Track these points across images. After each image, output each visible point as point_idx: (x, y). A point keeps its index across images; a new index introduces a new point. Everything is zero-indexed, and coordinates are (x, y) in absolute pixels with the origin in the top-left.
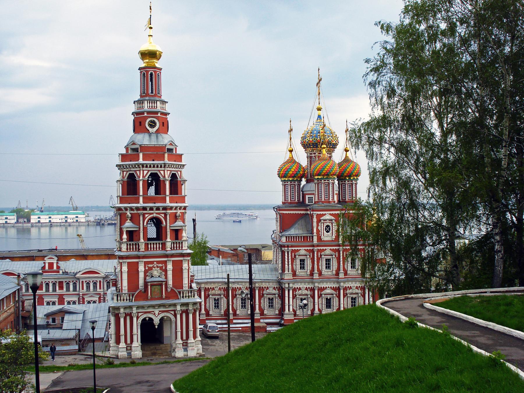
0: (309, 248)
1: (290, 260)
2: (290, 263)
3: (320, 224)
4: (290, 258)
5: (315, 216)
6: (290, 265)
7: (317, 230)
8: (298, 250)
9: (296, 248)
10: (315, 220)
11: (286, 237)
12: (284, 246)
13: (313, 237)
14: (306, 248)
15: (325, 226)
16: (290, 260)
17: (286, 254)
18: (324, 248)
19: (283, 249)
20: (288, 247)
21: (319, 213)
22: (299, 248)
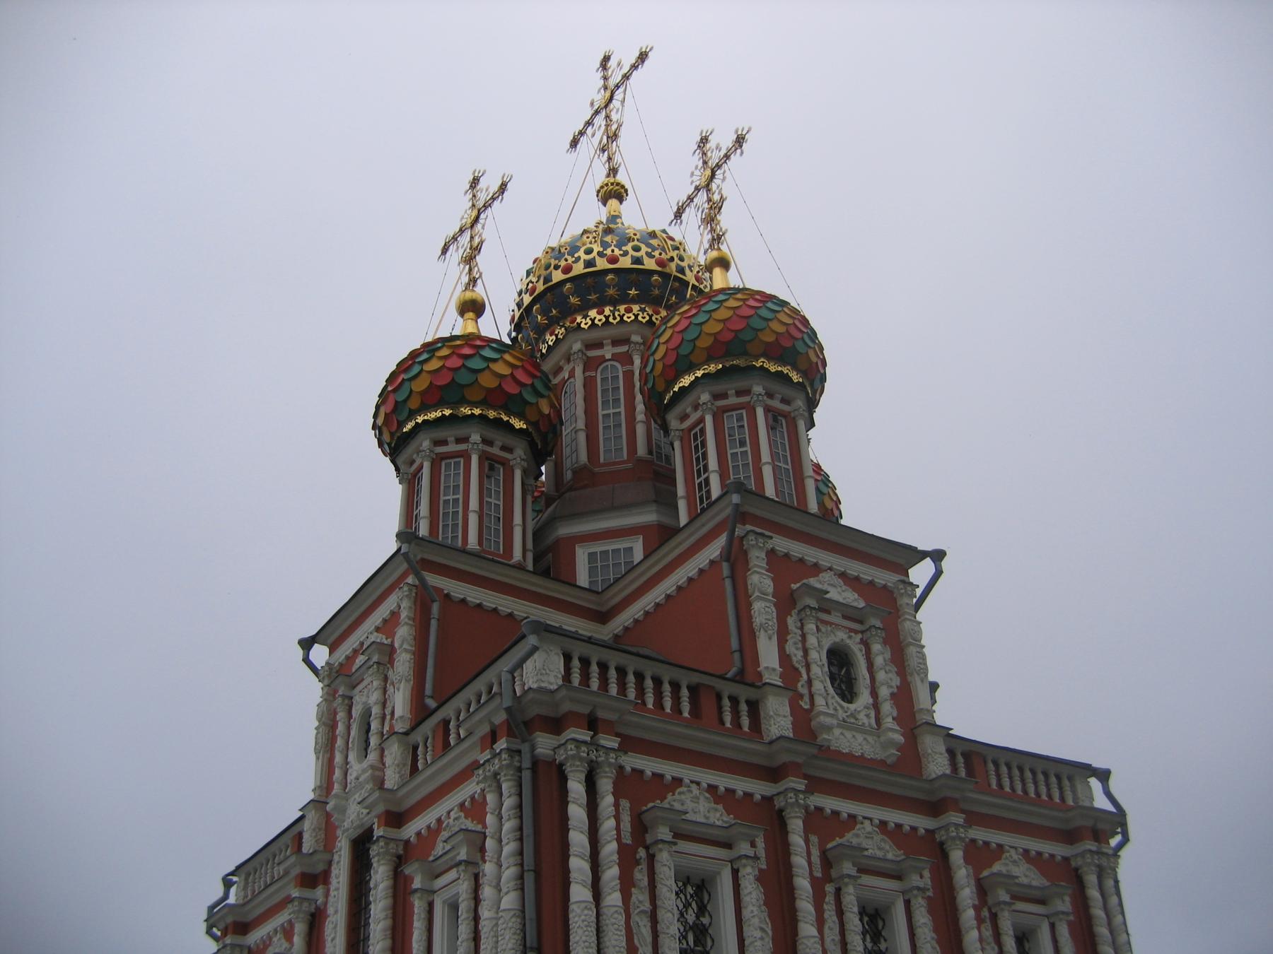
0: (742, 785)
1: (610, 849)
2: (611, 873)
3: (791, 621)
4: (608, 825)
5: (757, 558)
6: (613, 898)
7: (784, 658)
8: (662, 786)
9: (650, 765)
10: (760, 580)
11: (568, 658)
12: (555, 725)
13: (754, 707)
14: (723, 781)
15: (827, 643)
16: (610, 849)
17: (576, 787)
18: (846, 807)
19: (544, 743)
20: (592, 724)
21: (782, 544)
22: (669, 769)
